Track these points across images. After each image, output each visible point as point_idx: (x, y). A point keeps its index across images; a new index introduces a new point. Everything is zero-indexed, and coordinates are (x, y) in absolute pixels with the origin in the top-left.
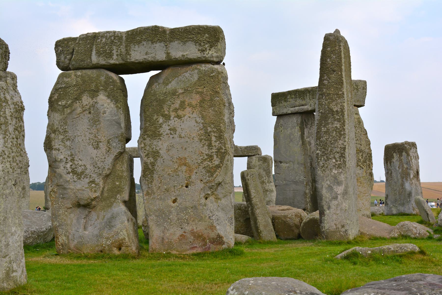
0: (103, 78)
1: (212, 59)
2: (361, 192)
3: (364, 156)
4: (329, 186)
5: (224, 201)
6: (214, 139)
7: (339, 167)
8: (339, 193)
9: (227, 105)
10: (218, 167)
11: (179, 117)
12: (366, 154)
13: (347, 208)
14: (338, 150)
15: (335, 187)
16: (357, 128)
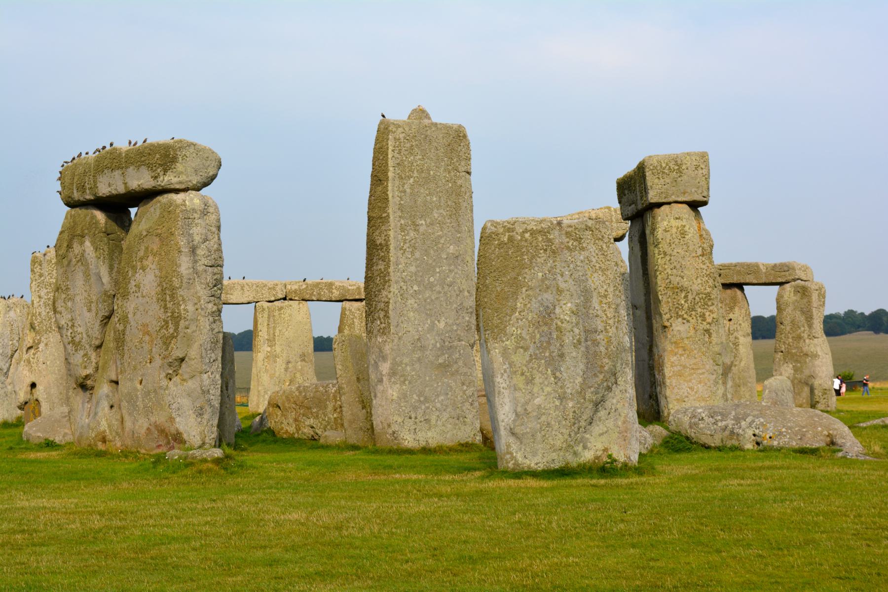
0: (88, 218)
1: (172, 187)
2: (685, 367)
3: (690, 297)
4: (376, 362)
5: (191, 384)
6: (168, 298)
7: (384, 333)
8: (384, 373)
9: (185, 250)
10: (173, 337)
11: (143, 269)
12: (695, 293)
13: (394, 397)
14: (382, 305)
15: (380, 364)
16: (673, 246)
